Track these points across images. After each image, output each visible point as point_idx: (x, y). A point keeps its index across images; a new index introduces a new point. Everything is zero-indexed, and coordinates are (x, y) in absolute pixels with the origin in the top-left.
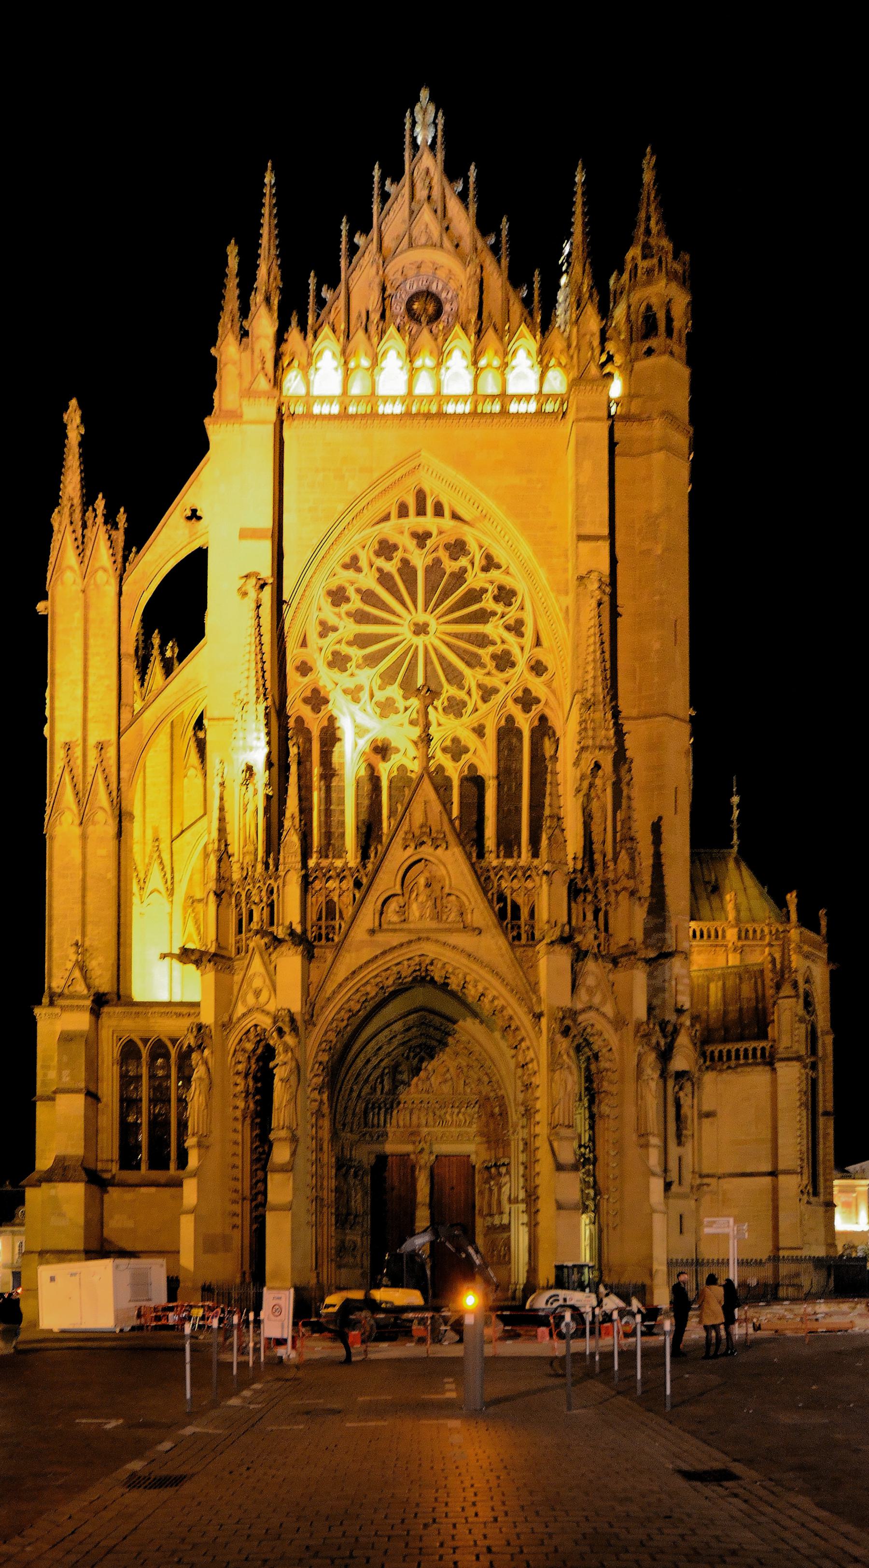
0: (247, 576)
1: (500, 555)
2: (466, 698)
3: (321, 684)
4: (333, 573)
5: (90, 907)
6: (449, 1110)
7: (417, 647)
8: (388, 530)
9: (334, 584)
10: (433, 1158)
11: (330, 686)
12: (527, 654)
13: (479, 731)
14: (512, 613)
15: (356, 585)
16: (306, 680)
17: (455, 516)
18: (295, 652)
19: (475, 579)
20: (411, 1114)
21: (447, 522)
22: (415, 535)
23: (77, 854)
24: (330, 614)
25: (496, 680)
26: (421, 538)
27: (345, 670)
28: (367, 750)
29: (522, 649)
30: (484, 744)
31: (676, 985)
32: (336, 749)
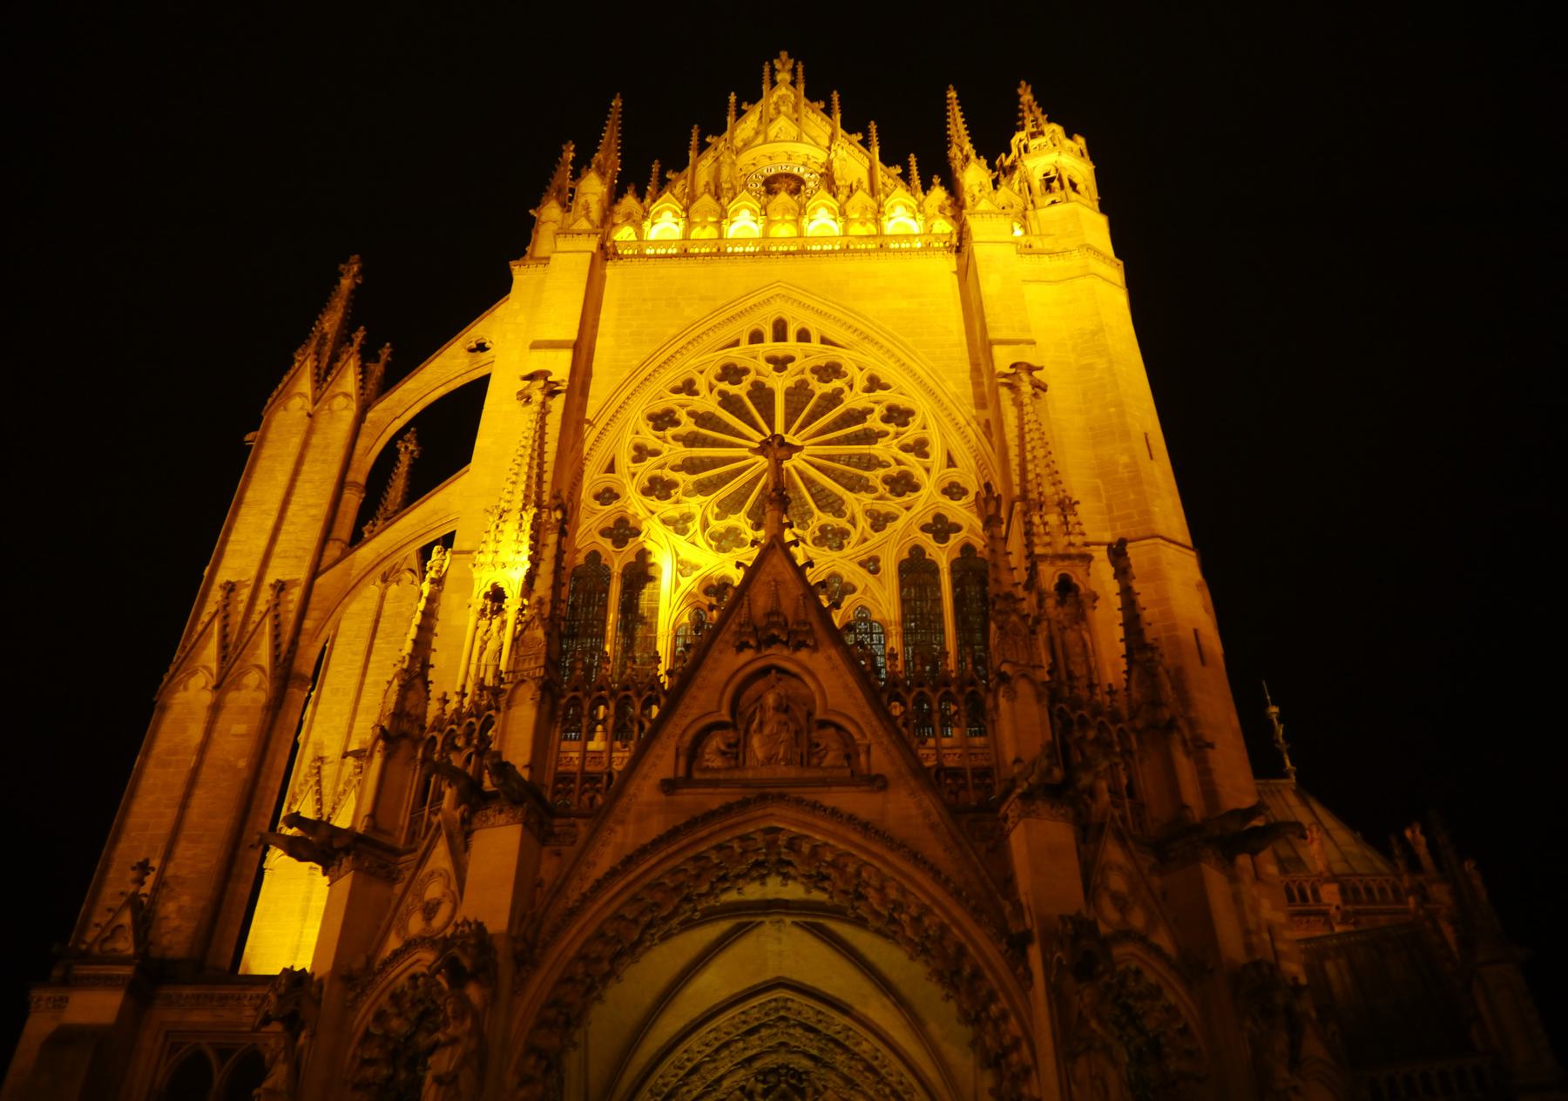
0: (531, 377)
1: (887, 373)
2: (849, 527)
3: (630, 511)
4: (659, 396)
5: (194, 814)
8: (736, 356)
9: (658, 408)
11: (642, 513)
12: (935, 474)
13: (871, 565)
14: (911, 433)
15: (689, 408)
16: (607, 508)
17: (824, 341)
18: (596, 476)
19: (855, 400)
21: (815, 344)
22: (771, 360)
23: (196, 733)
24: (650, 438)
25: (893, 504)
26: (780, 364)
27: (668, 497)
28: (695, 590)
29: (928, 470)
30: (879, 580)
31: (1272, 940)
32: (647, 591)
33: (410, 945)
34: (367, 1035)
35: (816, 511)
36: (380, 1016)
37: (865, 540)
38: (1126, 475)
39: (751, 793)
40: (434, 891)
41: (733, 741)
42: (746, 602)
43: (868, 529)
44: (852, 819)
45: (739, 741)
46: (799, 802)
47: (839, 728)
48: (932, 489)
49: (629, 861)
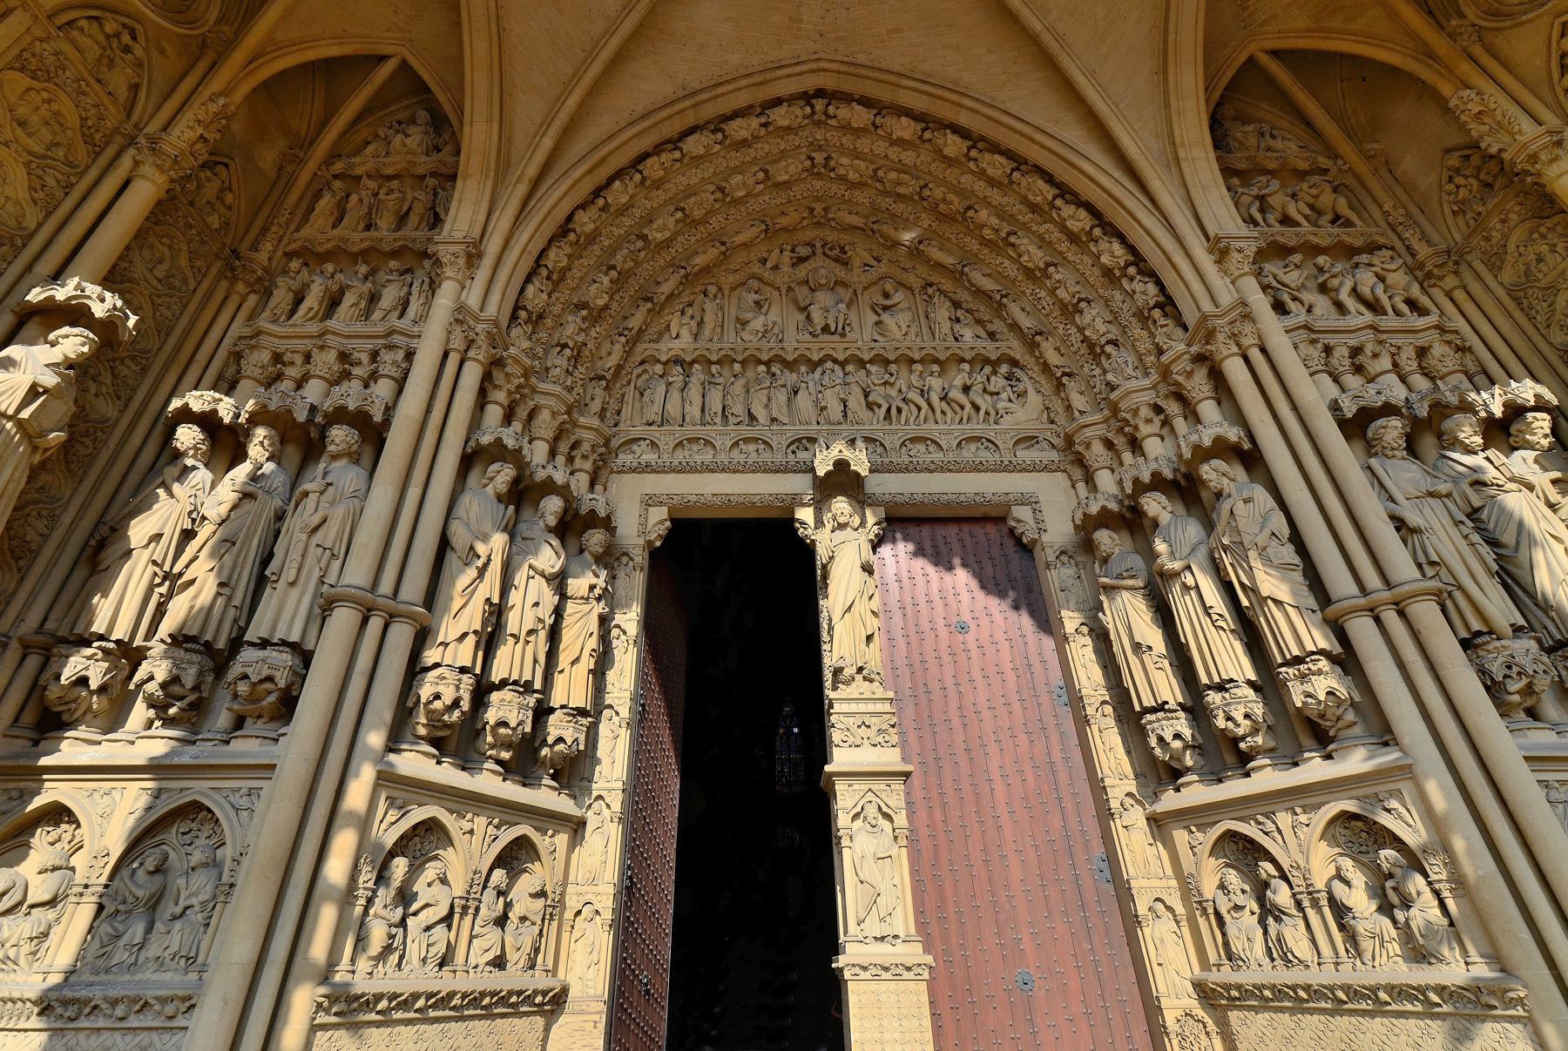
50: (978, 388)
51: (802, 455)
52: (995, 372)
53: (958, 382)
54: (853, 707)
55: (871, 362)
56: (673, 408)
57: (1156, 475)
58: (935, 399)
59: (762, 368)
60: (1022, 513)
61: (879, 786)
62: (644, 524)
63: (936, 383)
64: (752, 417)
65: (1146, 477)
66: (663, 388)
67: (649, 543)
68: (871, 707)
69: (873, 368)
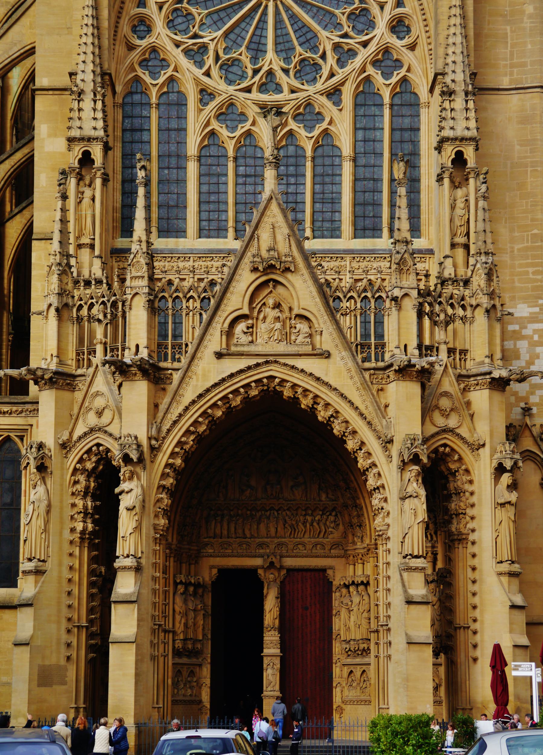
6: (302, 518)
7: (266, 7)
10: (284, 572)
16: (144, 43)
20: (259, 524)
29: (382, 8)
33: (92, 430)
34: (75, 470)
35: (299, 49)
36: (81, 460)
37: (332, 75)
38: (528, 25)
39: (260, 361)
40: (99, 402)
41: (249, 325)
42: (256, 239)
43: (335, 67)
44: (311, 374)
45: (253, 325)
46: (285, 365)
47: (307, 319)
48: (384, 29)
49: (200, 396)
50: (324, 521)
51: (261, 551)
52: (330, 514)
53: (317, 519)
54: (270, 638)
55: (288, 509)
56: (218, 531)
57: (353, 582)
58: (308, 525)
59: (249, 512)
60: (330, 572)
61: (274, 658)
62: (210, 573)
63: (309, 518)
64: (244, 534)
65: (351, 582)
66: (214, 522)
67: (212, 582)
68: (274, 638)
69: (288, 513)
